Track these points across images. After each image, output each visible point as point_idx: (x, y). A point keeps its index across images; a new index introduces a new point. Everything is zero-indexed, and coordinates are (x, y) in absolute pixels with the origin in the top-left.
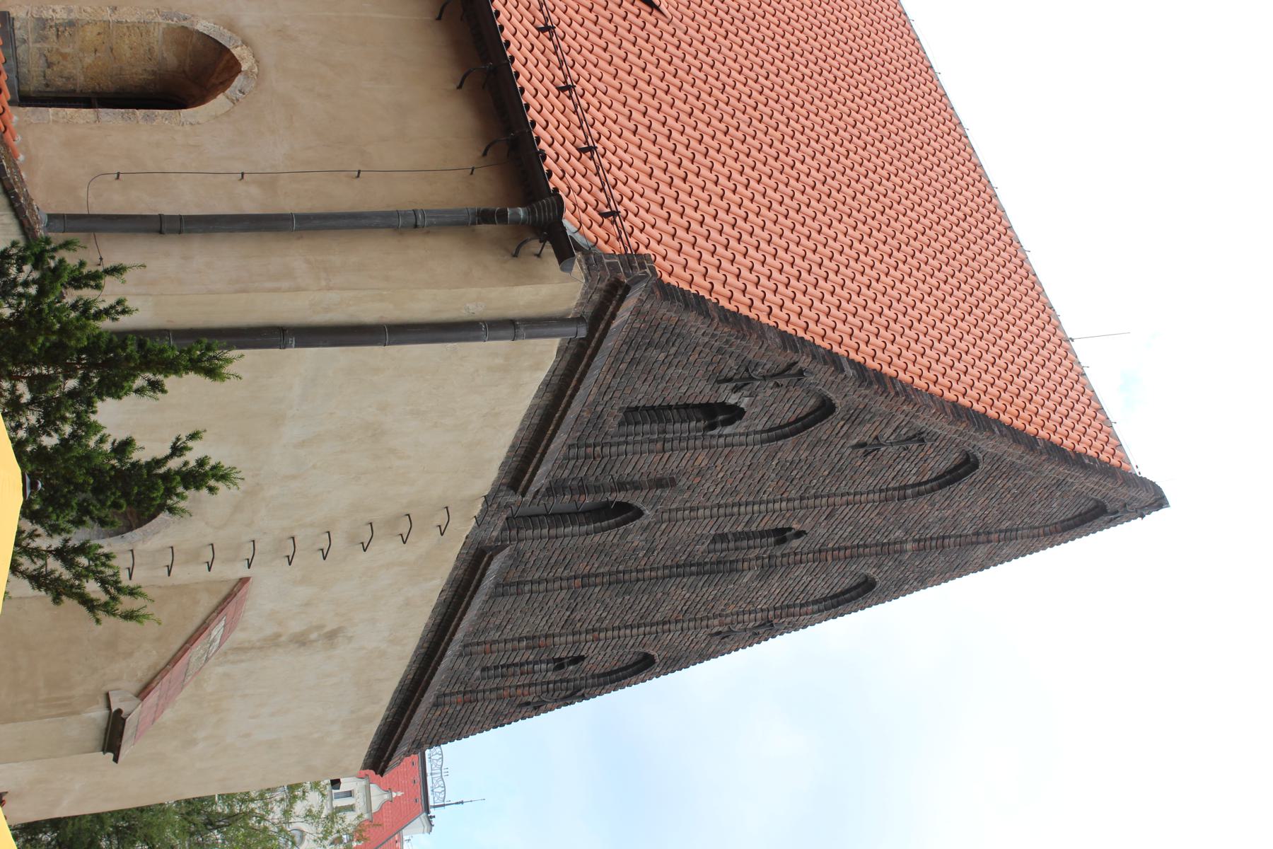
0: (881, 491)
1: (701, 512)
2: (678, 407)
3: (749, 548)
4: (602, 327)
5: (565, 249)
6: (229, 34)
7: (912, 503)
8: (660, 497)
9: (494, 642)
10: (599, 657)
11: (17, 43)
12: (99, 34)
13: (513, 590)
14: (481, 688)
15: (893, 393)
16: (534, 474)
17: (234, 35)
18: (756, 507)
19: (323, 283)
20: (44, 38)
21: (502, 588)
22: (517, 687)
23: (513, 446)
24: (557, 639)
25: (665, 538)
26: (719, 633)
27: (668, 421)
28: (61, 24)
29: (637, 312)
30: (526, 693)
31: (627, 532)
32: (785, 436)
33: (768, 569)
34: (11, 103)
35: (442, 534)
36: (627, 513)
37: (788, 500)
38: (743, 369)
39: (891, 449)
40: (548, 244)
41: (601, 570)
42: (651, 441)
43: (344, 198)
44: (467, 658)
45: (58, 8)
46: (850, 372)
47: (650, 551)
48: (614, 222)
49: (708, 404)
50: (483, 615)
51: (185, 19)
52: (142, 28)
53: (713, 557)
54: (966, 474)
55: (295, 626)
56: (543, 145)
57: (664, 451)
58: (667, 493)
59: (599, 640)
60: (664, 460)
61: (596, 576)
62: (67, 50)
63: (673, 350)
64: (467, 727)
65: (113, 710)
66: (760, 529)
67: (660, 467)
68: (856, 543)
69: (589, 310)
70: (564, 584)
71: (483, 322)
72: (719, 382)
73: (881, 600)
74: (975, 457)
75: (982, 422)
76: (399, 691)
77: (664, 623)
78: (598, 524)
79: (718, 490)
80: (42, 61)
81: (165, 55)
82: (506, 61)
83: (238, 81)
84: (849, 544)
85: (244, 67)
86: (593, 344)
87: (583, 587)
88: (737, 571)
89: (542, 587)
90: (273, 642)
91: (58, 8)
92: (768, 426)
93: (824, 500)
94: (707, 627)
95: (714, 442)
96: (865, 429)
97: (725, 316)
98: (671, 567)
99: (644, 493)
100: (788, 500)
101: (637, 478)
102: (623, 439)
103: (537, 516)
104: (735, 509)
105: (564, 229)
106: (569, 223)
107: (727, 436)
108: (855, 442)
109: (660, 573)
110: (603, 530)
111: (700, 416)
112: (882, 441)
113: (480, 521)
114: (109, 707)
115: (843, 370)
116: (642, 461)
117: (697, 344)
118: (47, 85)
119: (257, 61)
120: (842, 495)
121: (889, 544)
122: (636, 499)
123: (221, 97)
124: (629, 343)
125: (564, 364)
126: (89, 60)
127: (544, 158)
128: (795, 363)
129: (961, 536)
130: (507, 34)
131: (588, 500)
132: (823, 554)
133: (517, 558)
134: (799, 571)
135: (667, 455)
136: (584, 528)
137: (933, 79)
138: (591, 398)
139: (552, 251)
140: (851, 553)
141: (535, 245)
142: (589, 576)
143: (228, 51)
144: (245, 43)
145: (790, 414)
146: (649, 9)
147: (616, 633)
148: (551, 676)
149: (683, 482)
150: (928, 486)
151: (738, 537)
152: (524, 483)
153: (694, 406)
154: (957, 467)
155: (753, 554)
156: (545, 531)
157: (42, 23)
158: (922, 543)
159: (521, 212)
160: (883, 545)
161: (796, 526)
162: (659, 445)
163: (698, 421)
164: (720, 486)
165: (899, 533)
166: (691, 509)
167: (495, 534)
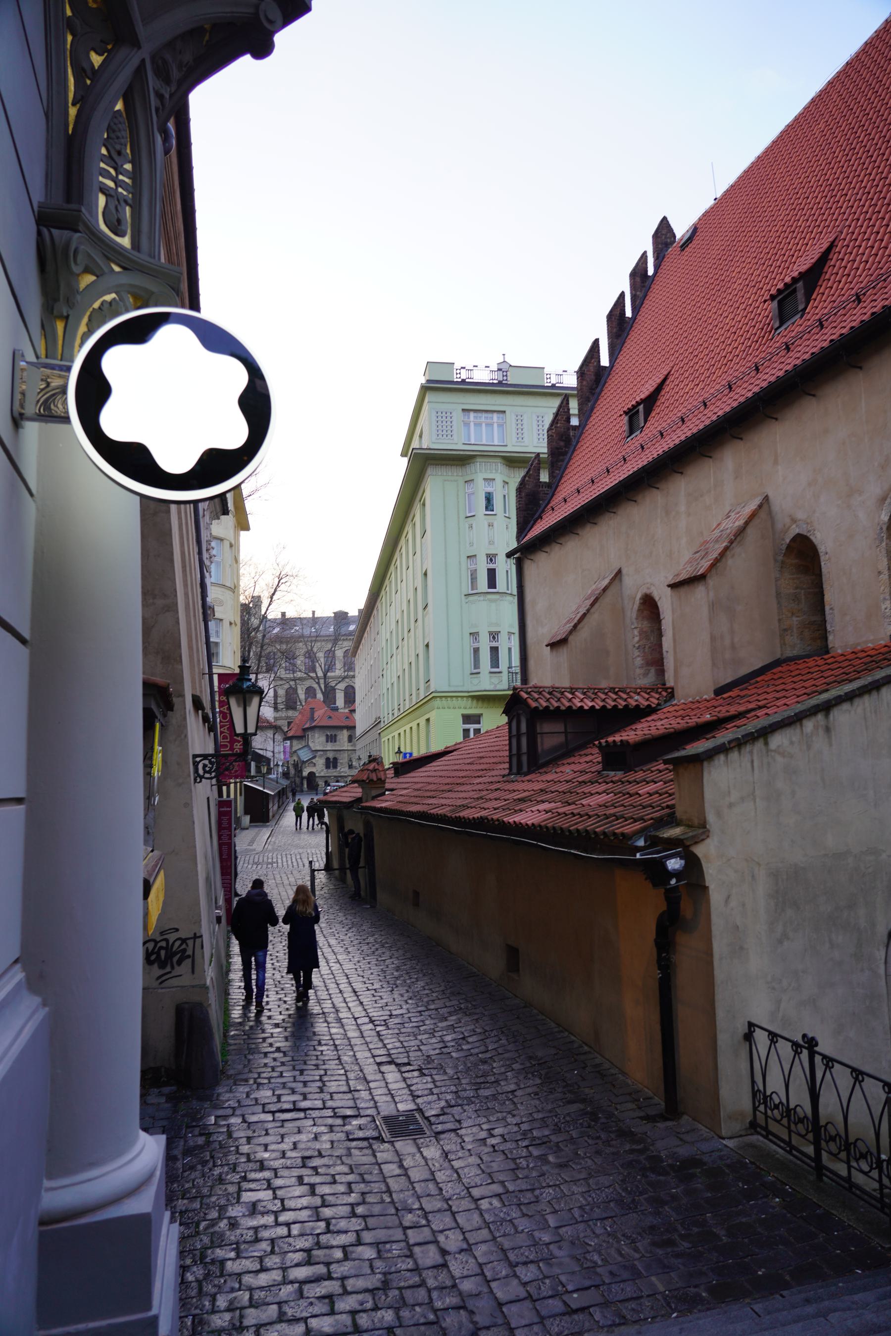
45: (883, 607)
51: (881, 529)
91: (883, 607)
146: (834, 248)
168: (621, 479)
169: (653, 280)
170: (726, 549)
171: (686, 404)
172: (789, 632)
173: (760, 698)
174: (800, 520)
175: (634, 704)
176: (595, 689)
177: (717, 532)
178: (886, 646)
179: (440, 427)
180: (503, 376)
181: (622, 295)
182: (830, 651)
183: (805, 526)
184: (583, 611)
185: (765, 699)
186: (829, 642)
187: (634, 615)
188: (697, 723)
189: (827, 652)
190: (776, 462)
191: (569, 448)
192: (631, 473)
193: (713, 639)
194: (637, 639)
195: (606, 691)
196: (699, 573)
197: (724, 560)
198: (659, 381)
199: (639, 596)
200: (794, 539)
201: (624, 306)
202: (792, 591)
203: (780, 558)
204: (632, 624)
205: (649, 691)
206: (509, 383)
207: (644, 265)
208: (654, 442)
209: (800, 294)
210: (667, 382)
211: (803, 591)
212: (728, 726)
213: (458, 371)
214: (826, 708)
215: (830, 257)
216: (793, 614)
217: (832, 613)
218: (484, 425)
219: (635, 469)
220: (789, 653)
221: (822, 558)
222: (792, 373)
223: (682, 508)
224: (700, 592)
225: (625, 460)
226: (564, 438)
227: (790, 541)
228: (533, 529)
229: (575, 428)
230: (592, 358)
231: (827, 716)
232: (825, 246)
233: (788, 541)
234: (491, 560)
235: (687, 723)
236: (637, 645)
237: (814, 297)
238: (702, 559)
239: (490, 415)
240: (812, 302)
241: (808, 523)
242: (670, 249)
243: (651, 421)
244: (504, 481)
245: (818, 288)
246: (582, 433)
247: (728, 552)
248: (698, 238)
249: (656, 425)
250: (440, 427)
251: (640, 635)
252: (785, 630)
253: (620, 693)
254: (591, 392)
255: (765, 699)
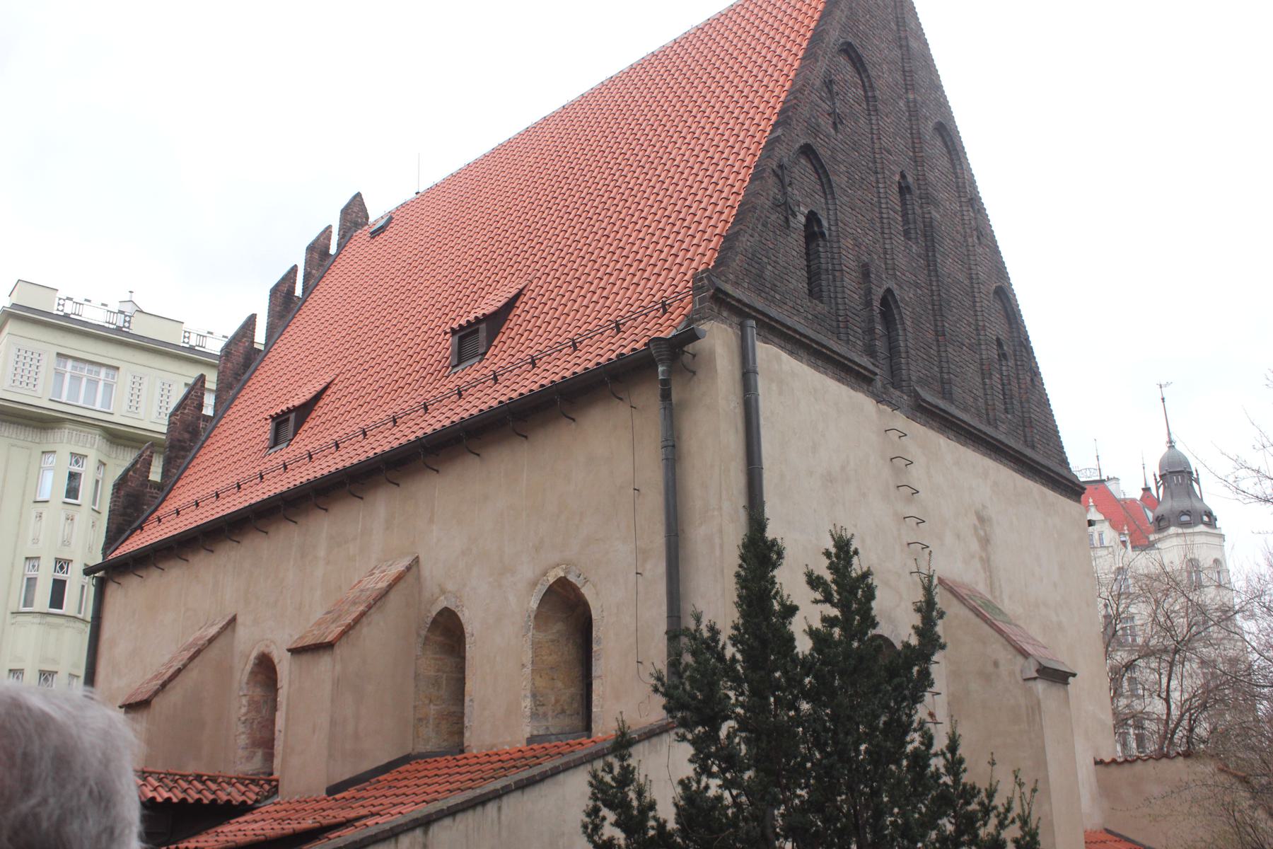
0: (869, 115)
1: (887, 246)
2: (808, 260)
3: (914, 213)
4: (747, 310)
5: (689, 336)
6: (539, 585)
7: (878, 92)
8: (876, 275)
9: (986, 403)
10: (997, 328)
11: (549, 733)
12: (541, 677)
13: (947, 386)
14: (1020, 414)
15: (795, 101)
16: (859, 365)
17: (540, 582)
18: (883, 206)
19: (716, 513)
20: (545, 715)
21: (947, 395)
22: (1020, 388)
23: (839, 381)
24: (984, 357)
25: (907, 274)
26: (978, 238)
27: (819, 268)
28: (535, 703)
29: (736, 284)
30: (1024, 381)
31: (903, 300)
32: (829, 180)
33: (928, 199)
34: (589, 737)
35: (906, 435)
36: (888, 300)
37: (878, 182)
38: (779, 209)
39: (838, 105)
40: (685, 349)
41: (932, 322)
42: (834, 280)
43: (654, 501)
44: (999, 423)
46: (779, 132)
47: (917, 285)
48: (670, 305)
49: (806, 237)
50: (965, 410)
51: (529, 616)
52: (536, 646)
53: (921, 241)
54: (855, 52)
55: (975, 546)
56: (613, 356)
57: (841, 270)
58: (873, 269)
59: (984, 326)
60: (848, 270)
61: (936, 326)
62: (553, 700)
63: (765, 260)
64: (1049, 425)
65: (1037, 675)
66: (899, 204)
67: (854, 274)
68: (909, 135)
69: (736, 320)
70: (942, 349)
71: (745, 396)
72: (788, 227)
73: (952, 119)
74: (842, 44)
75: (817, 37)
76: (1022, 473)
77: (971, 278)
78: (897, 322)
79: (871, 234)
80: (561, 717)
81: (554, 631)
82: (555, 387)
83: (572, 578)
84: (910, 141)
85: (562, 574)
86: (761, 317)
87: (944, 335)
88: (931, 222)
89: (945, 365)
90: (986, 563)
91: (523, 705)
92: (822, 194)
93: (877, 156)
94: (974, 246)
95: (834, 234)
96: (822, 123)
97: (738, 221)
98: (929, 270)
99: (874, 287)
100: (878, 182)
101: (862, 292)
102: (833, 301)
103: (891, 367)
104: (885, 221)
105: (674, 336)
106: (668, 333)
107: (830, 225)
108: (833, 131)
109: (934, 279)
110: (902, 318)
111: (814, 245)
112: (831, 111)
113: (895, 407)
114: (1035, 679)
115: (778, 136)
116: (849, 287)
117: (760, 241)
118: (578, 714)
119: (558, 565)
120: (873, 143)
121: (909, 111)
122: (878, 293)
123: (583, 590)
124: (759, 291)
125: (776, 340)
126: (560, 685)
127: (623, 354)
128: (773, 171)
129: (903, 59)
130: (535, 387)
131: (879, 328)
132: (918, 159)
133: (923, 382)
134: (931, 177)
135: (844, 268)
136: (901, 332)
137: (572, 104)
138: (802, 321)
139: (691, 345)
140: (916, 140)
141: (686, 358)
142: (936, 332)
143: (551, 586)
144: (545, 574)
145: (812, 178)
147: (979, 313)
148: (1012, 363)
149: (865, 258)
150: (866, 80)
151: (906, 221)
152: (866, 373)
153: (807, 248)
154: (851, 58)
155: (918, 211)
156: (903, 361)
157: (534, 715)
158: (909, 87)
159: (660, 369)
160: (910, 115)
161: (897, 178)
162: (837, 274)
163: (818, 245)
164: (868, 231)
165: (901, 104)
166: (885, 253)
167: (905, 397)
168: (253, 501)
169: (334, 261)
170: (363, 614)
171: (345, 425)
172: (425, 722)
173: (376, 802)
174: (449, 592)
175: (225, 798)
176: (176, 774)
177: (356, 590)
178: (520, 751)
179: (19, 371)
180: (125, 321)
181: (294, 269)
182: (466, 751)
183: (453, 600)
184: (177, 665)
185: (381, 804)
186: (465, 740)
187: (245, 678)
188: (294, 830)
189: (462, 751)
190: (431, 521)
191: (195, 443)
192: (265, 497)
193: (333, 723)
194: (244, 710)
195: (191, 778)
196: (326, 640)
197: (358, 627)
198: (319, 388)
199: (254, 654)
200: (441, 613)
201: (294, 283)
202: (432, 673)
203: (424, 633)
204: (241, 689)
205: (247, 782)
206: (131, 331)
207: (326, 241)
208: (299, 464)
209: (483, 334)
210: (329, 392)
211: (445, 676)
212: (331, 836)
213: (62, 302)
214: (425, 823)
215: (517, 305)
216: (431, 701)
217: (470, 706)
218: (84, 380)
219: (272, 494)
220: (421, 748)
221: (468, 640)
222: (458, 426)
223: (322, 553)
224: (324, 665)
225: (262, 477)
226: (190, 429)
227: (437, 615)
228: (128, 542)
229: (207, 418)
230: (244, 336)
231: (426, 833)
232: (514, 291)
233: (434, 614)
234: (61, 567)
235: (283, 829)
236: (243, 719)
237: (495, 343)
238: (333, 622)
239: (95, 368)
240: (493, 347)
241: (457, 597)
242: (360, 231)
243: (302, 434)
244: (100, 461)
245: (501, 334)
246: (215, 427)
247: (364, 619)
248: (392, 230)
249: (306, 442)
250: (19, 371)
251: (249, 705)
252: (420, 720)
253: (209, 783)
254: (235, 378)
255: (381, 804)
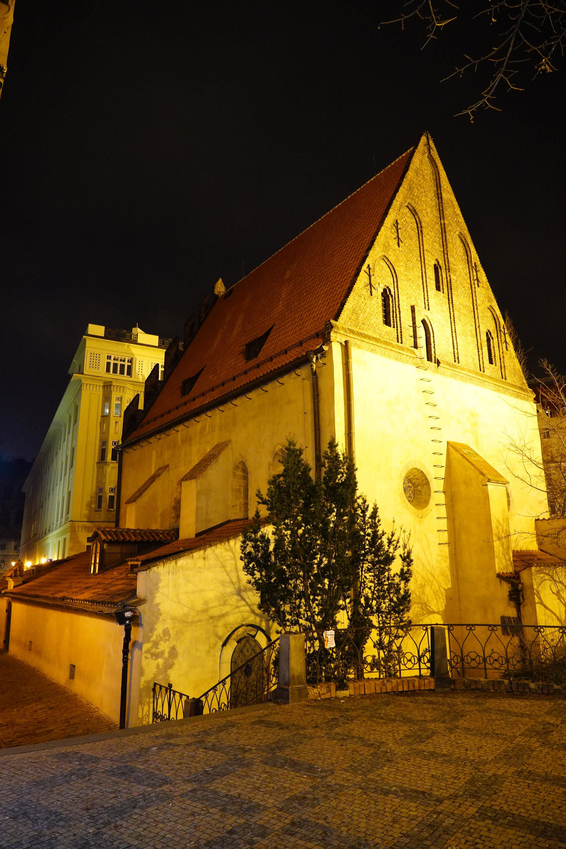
108: (397, 246)
150: (417, 219)
179: (92, 362)
193: (197, 508)
216: (237, 499)
250: (92, 362)
